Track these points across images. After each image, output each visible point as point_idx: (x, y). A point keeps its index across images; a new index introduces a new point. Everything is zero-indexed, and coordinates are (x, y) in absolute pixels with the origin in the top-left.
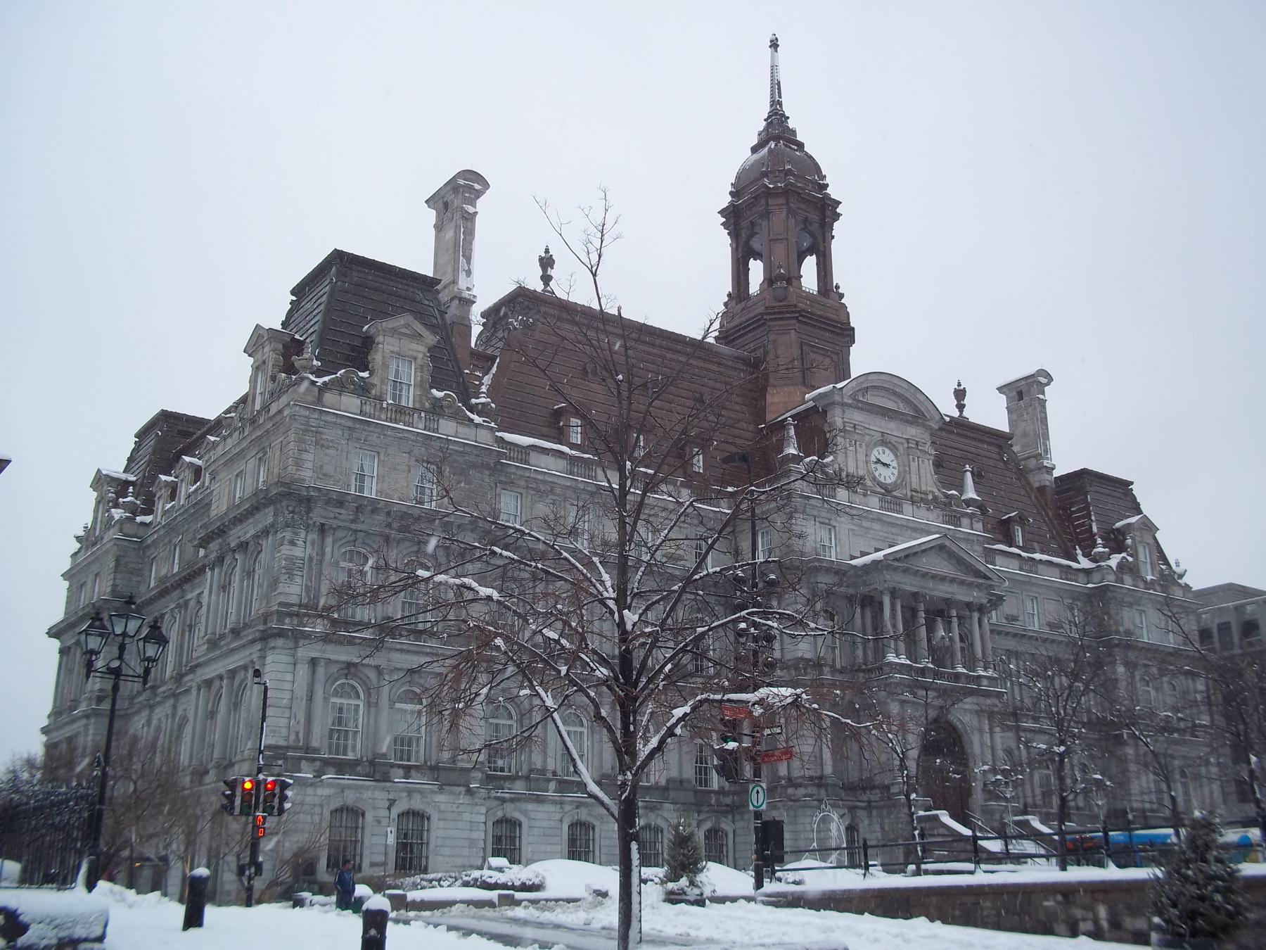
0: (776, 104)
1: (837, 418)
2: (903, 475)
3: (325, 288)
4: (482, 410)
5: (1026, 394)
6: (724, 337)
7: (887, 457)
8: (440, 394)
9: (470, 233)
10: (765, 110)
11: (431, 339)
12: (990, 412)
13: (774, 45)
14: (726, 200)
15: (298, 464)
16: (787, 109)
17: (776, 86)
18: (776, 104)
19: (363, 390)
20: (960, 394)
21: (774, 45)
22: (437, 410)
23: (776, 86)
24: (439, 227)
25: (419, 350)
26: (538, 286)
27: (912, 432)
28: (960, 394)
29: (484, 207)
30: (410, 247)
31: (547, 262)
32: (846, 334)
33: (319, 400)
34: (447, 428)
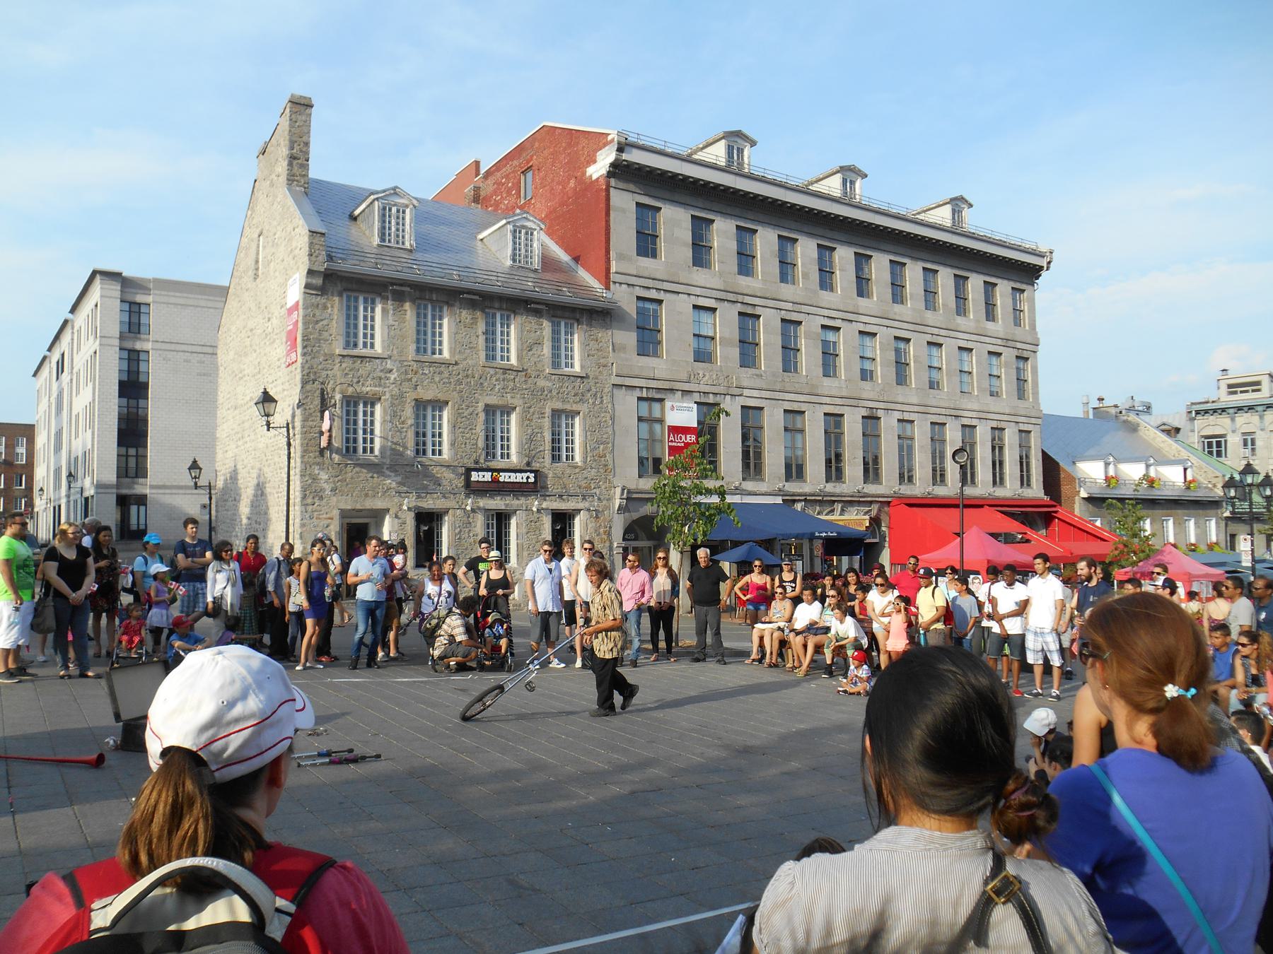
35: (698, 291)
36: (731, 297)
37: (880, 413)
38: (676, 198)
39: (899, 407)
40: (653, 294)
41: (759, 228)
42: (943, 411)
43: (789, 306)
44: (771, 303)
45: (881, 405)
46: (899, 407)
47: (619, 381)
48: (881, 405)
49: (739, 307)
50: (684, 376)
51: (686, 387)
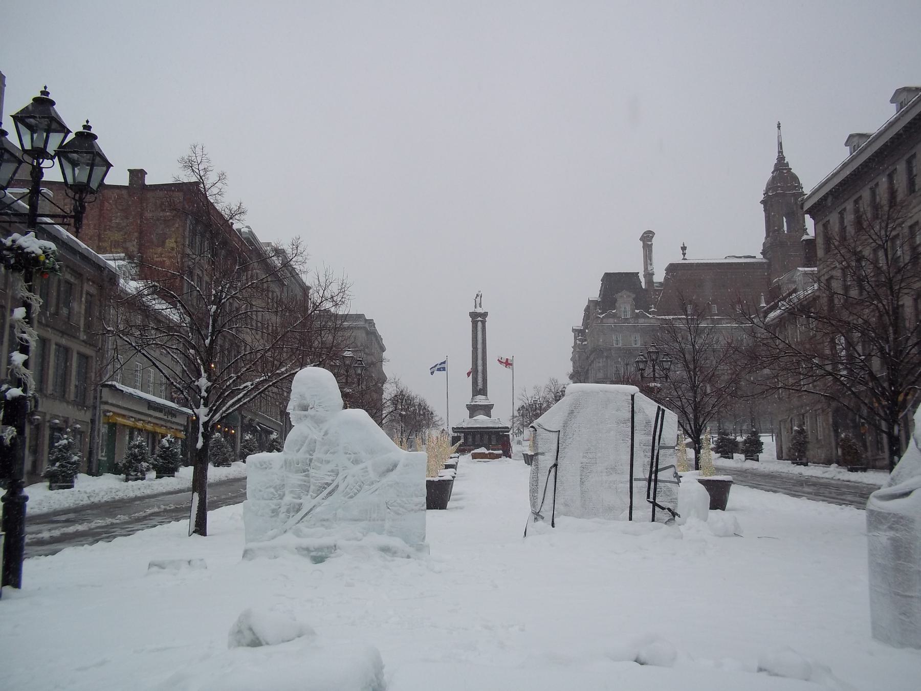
0: (781, 152)
4: (653, 313)
8: (637, 311)
9: (651, 251)
11: (634, 296)
13: (779, 127)
14: (762, 197)
15: (598, 341)
17: (780, 144)
18: (781, 152)
19: (614, 316)
21: (779, 127)
22: (637, 316)
23: (780, 144)
25: (631, 299)
26: (678, 259)
29: (655, 241)
30: (632, 263)
31: (684, 248)
33: (602, 322)
34: (641, 320)
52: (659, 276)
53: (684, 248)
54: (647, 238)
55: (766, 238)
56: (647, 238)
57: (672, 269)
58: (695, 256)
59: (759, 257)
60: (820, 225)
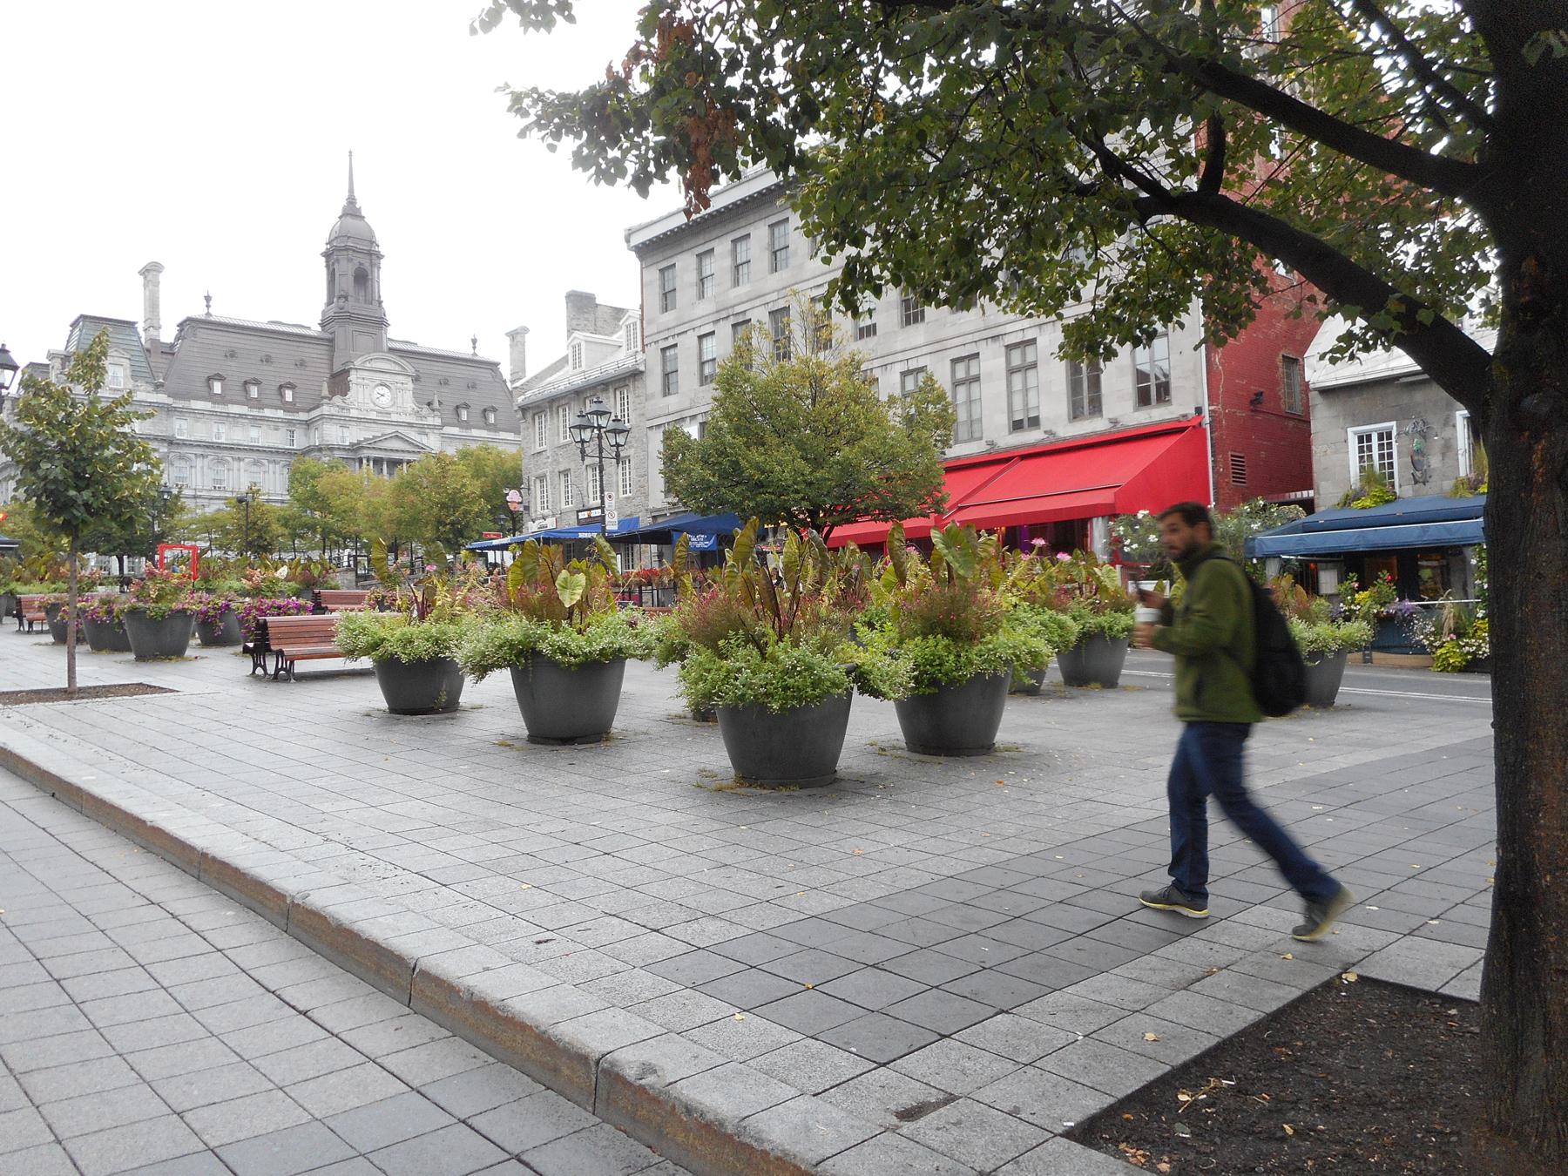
0: (351, 190)
1: (353, 377)
2: (394, 400)
3: (77, 332)
5: (516, 337)
6: (322, 325)
7: (384, 390)
10: (346, 195)
12: (495, 350)
14: (323, 248)
16: (357, 194)
18: (351, 190)
20: (474, 341)
24: (145, 286)
27: (400, 378)
28: (474, 341)
29: (162, 277)
30: (126, 305)
31: (208, 299)
32: (381, 323)
35: (698, 323)
36: (724, 314)
37: (877, 373)
38: (686, 246)
39: (900, 357)
40: (671, 342)
41: (751, 230)
42: (969, 338)
43: (774, 296)
44: (757, 302)
45: (876, 363)
46: (900, 357)
47: (649, 424)
48: (876, 363)
49: (732, 320)
50: (687, 405)
51: (691, 413)
52: (168, 335)
53: (208, 299)
54: (151, 272)
55: (330, 303)
56: (151, 272)
57: (189, 326)
58: (220, 312)
59: (316, 329)
60: (653, 274)
